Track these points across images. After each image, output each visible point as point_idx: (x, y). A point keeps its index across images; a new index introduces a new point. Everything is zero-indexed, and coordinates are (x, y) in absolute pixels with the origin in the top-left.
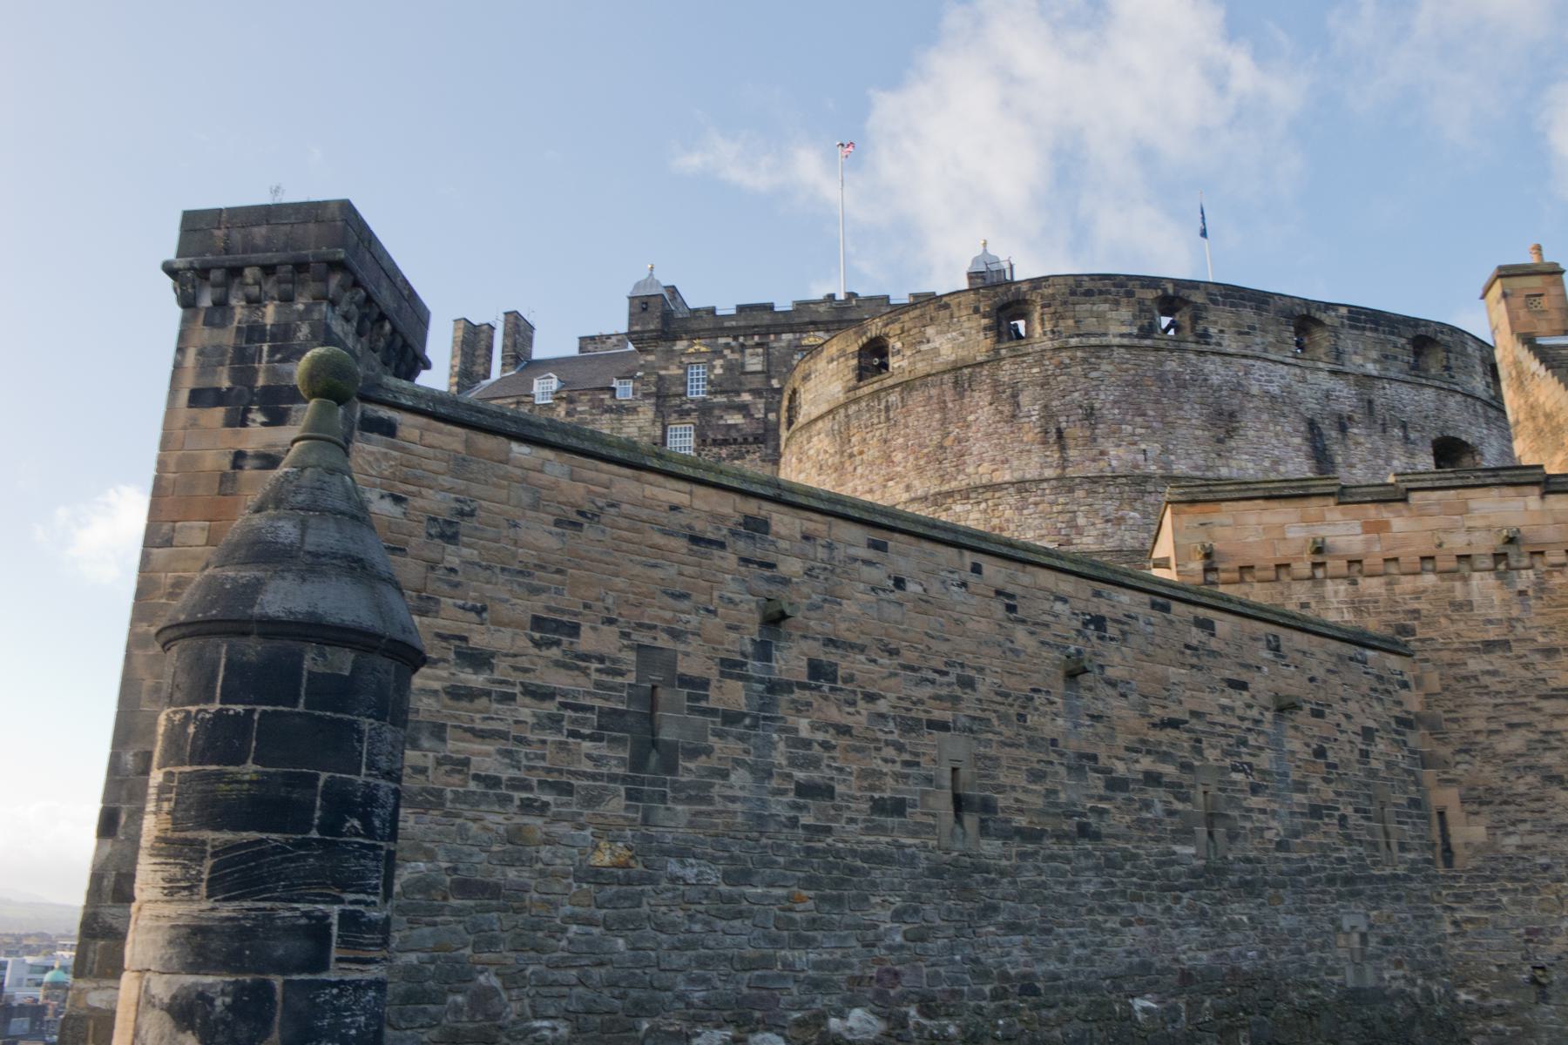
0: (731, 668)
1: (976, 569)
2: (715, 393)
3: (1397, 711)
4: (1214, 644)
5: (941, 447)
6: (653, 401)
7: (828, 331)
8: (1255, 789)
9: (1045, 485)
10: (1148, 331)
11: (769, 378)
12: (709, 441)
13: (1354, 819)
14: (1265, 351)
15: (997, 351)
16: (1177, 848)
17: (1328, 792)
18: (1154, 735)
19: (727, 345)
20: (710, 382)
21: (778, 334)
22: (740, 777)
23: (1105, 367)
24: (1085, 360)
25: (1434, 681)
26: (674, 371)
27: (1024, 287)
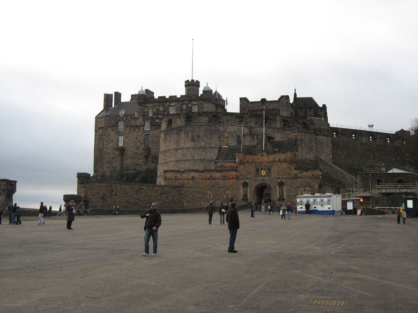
0: (109, 194)
1: (129, 186)
2: (154, 115)
3: (180, 193)
4: (154, 189)
5: (177, 140)
6: (142, 117)
7: (176, 102)
8: (157, 201)
9: (191, 148)
10: (209, 122)
11: (164, 112)
12: (153, 125)
13: (170, 203)
14: (231, 124)
15: (186, 125)
16: (147, 205)
17: (167, 201)
18: (145, 197)
19: (156, 105)
20: (153, 113)
21: (166, 103)
22: (109, 201)
23: (202, 128)
24: (199, 127)
25: (185, 190)
26: (146, 110)
27: (191, 114)
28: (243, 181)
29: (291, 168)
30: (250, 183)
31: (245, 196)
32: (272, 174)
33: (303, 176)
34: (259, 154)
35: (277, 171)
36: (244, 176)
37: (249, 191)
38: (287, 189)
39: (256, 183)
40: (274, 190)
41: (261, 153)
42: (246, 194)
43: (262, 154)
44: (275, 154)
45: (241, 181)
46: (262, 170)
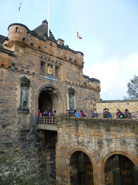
28: (22, 76)
29: (80, 73)
30: (33, 81)
31: (25, 103)
32: (61, 76)
33: (90, 87)
34: (47, 42)
35: (67, 73)
36: (24, 68)
37: (30, 95)
38: (77, 99)
39: (42, 83)
40: (64, 99)
41: (50, 42)
42: (27, 100)
43: (51, 43)
44: (66, 50)
45: (18, 74)
46: (49, 65)
